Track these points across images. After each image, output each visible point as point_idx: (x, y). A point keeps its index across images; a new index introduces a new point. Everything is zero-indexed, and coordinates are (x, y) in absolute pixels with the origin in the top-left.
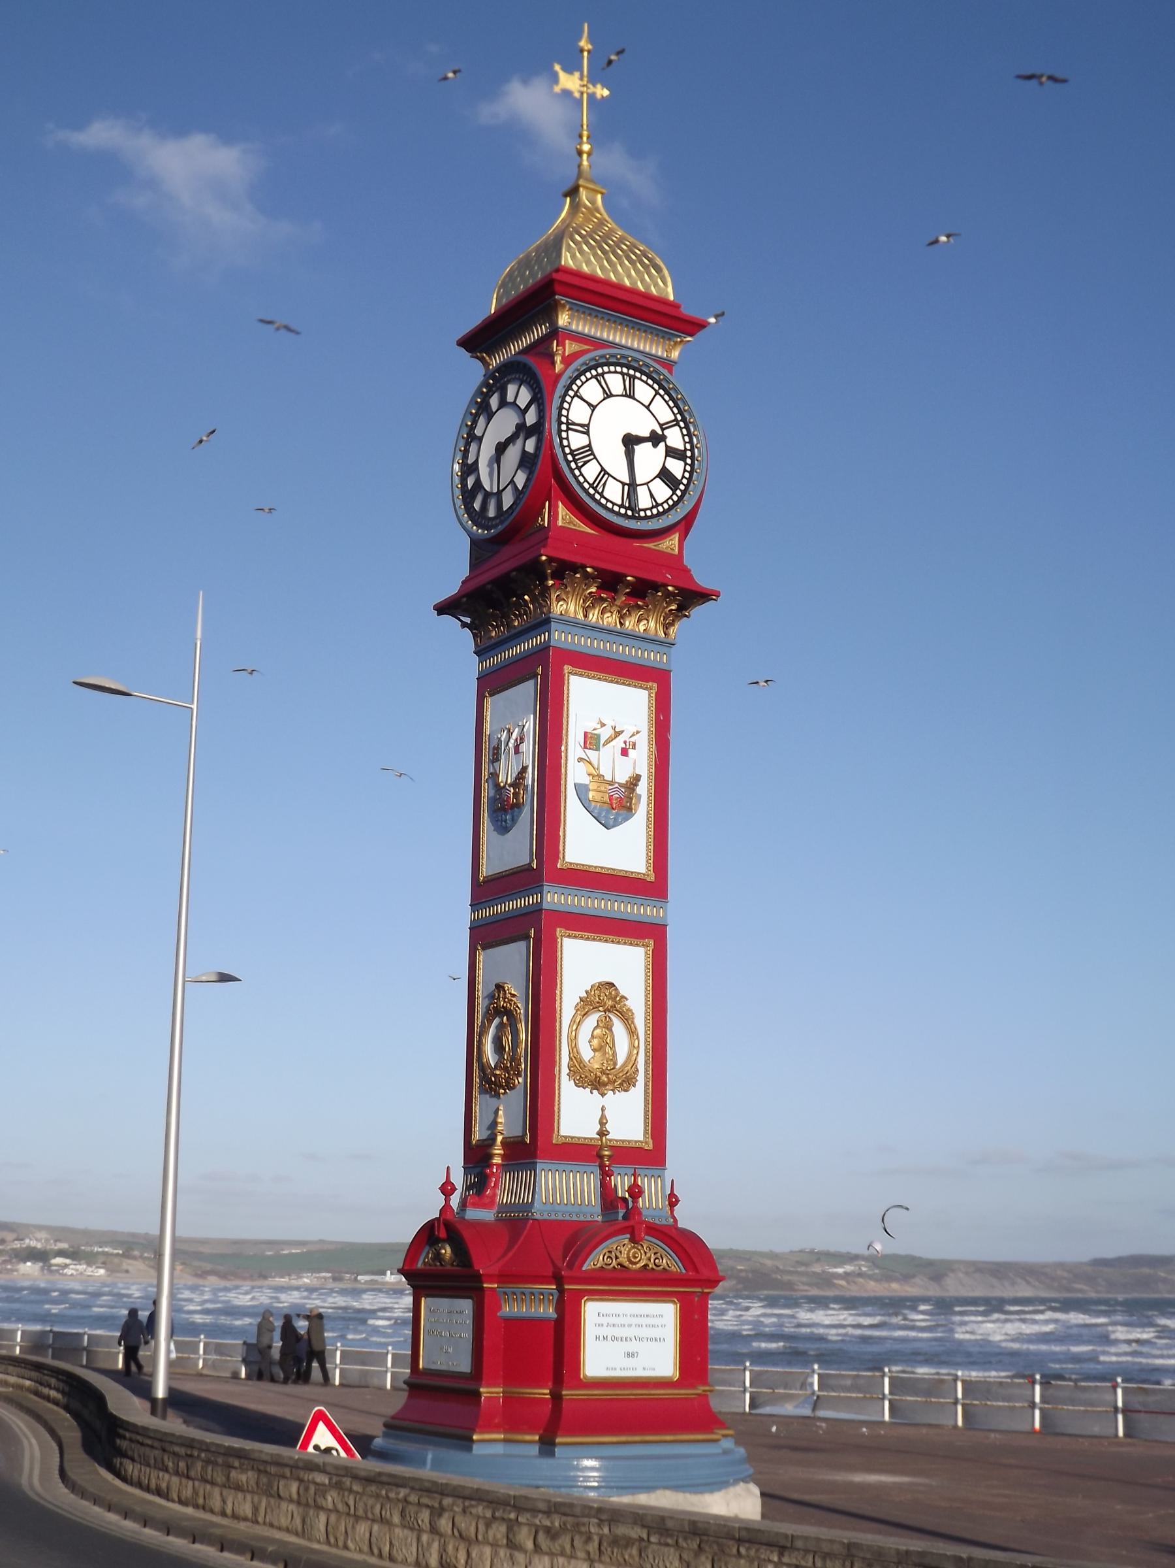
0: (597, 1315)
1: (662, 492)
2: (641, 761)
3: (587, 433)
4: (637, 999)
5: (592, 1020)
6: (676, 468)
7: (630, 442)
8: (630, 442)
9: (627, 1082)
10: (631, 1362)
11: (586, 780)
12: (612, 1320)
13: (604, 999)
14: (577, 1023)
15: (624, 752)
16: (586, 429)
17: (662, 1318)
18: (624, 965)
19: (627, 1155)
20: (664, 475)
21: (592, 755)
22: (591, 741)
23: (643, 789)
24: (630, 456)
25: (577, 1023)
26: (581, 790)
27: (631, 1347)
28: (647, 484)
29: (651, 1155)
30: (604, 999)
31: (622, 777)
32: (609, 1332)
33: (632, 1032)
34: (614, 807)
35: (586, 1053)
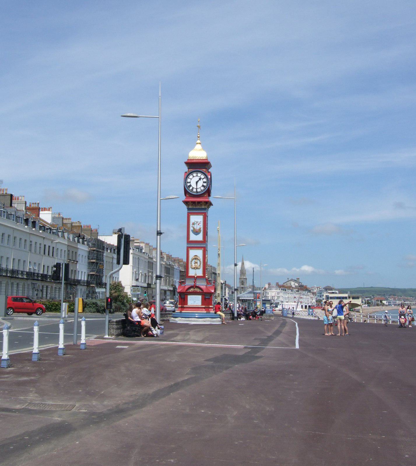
0: (190, 297)
1: (202, 188)
2: (201, 226)
3: (190, 183)
5: (194, 261)
6: (205, 184)
9: (199, 269)
11: (192, 229)
12: (192, 298)
13: (196, 258)
14: (191, 262)
15: (199, 224)
16: (190, 182)
17: (200, 297)
18: (199, 253)
20: (203, 186)
21: (194, 226)
22: (193, 224)
23: (202, 229)
24: (197, 184)
25: (191, 262)
26: (192, 230)
27: (194, 301)
28: (200, 188)
31: (198, 228)
32: (192, 299)
33: (200, 262)
34: (196, 233)
35: (193, 265)
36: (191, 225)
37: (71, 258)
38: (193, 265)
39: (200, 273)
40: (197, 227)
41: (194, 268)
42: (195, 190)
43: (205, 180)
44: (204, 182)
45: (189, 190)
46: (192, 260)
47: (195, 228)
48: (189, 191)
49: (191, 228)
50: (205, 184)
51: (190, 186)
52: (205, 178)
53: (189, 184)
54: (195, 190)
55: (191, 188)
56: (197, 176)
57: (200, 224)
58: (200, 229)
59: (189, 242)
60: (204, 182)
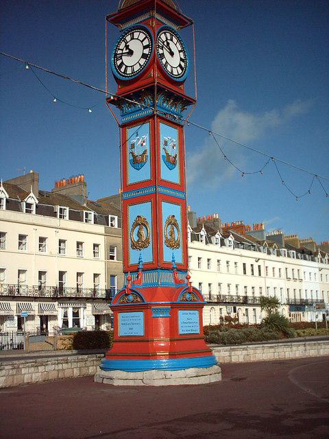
1: (143, 61)
2: (147, 145)
4: (149, 220)
6: (147, 51)
7: (131, 53)
8: (131, 53)
10: (131, 331)
14: (133, 230)
15: (142, 145)
19: (149, 268)
20: (144, 56)
29: (184, 268)
30: (140, 223)
34: (137, 162)
36: (129, 151)
37: (296, 277)
38: (136, 238)
39: (147, 255)
40: (138, 152)
41: (134, 246)
42: (129, 71)
43: (146, 42)
44: (145, 47)
45: (120, 74)
46: (136, 224)
47: (136, 154)
48: (121, 78)
49: (129, 157)
50: (147, 51)
51: (122, 63)
52: (146, 37)
53: (119, 62)
54: (129, 71)
55: (123, 70)
56: (133, 38)
57: (144, 144)
58: (145, 152)
59: (127, 188)
60: (145, 47)
